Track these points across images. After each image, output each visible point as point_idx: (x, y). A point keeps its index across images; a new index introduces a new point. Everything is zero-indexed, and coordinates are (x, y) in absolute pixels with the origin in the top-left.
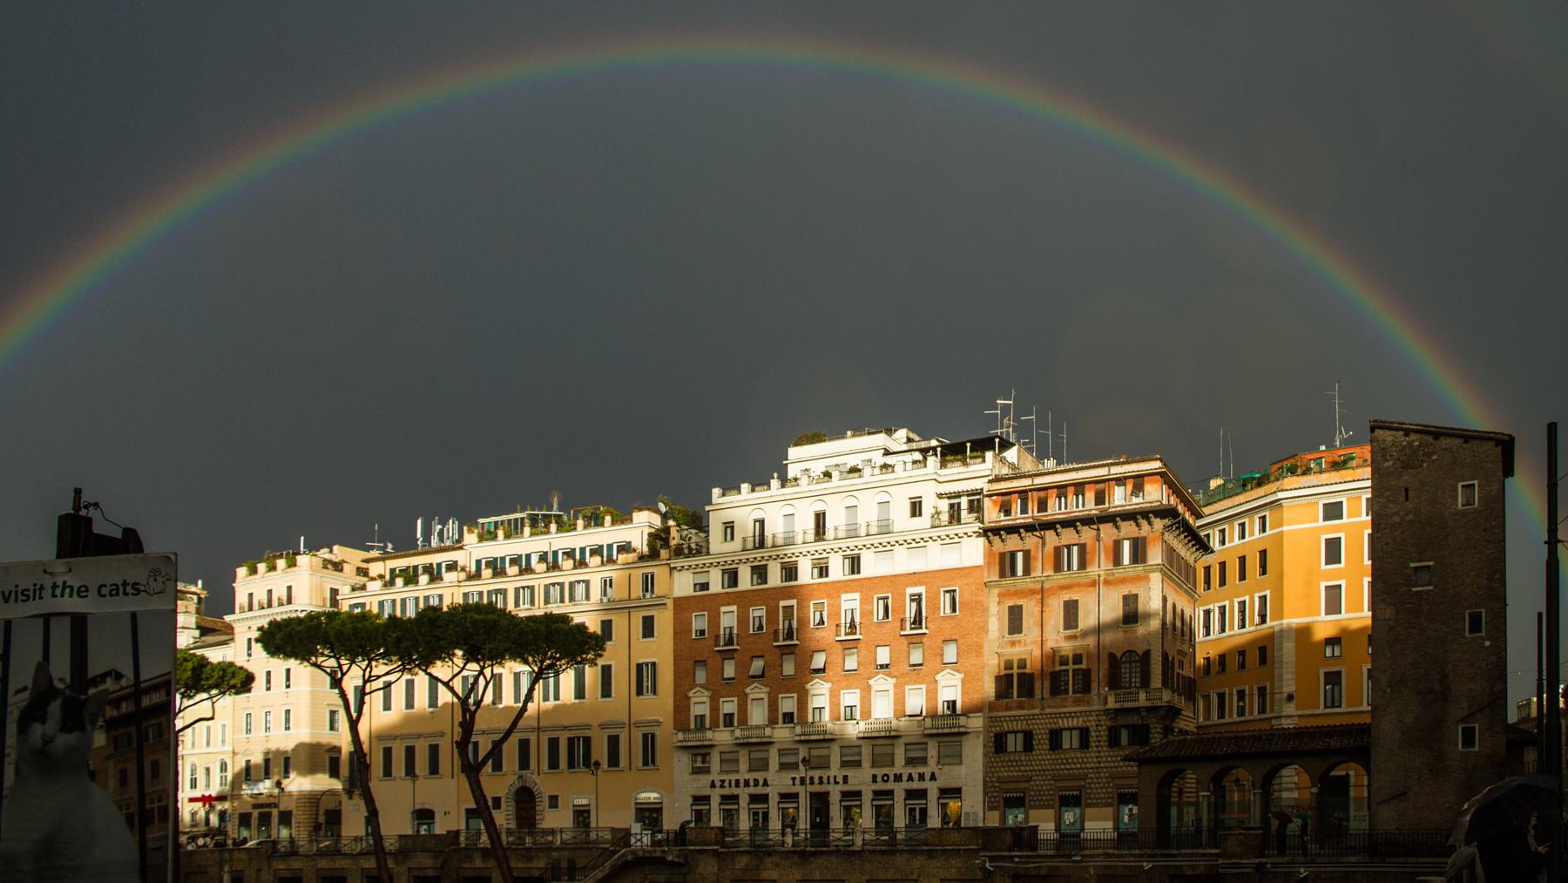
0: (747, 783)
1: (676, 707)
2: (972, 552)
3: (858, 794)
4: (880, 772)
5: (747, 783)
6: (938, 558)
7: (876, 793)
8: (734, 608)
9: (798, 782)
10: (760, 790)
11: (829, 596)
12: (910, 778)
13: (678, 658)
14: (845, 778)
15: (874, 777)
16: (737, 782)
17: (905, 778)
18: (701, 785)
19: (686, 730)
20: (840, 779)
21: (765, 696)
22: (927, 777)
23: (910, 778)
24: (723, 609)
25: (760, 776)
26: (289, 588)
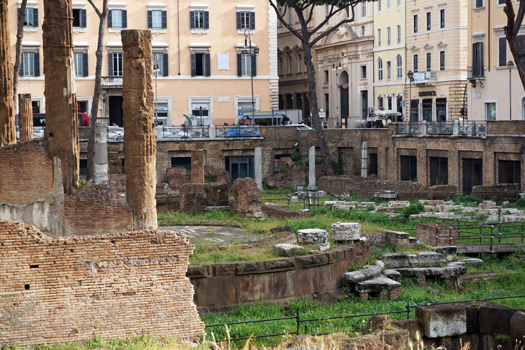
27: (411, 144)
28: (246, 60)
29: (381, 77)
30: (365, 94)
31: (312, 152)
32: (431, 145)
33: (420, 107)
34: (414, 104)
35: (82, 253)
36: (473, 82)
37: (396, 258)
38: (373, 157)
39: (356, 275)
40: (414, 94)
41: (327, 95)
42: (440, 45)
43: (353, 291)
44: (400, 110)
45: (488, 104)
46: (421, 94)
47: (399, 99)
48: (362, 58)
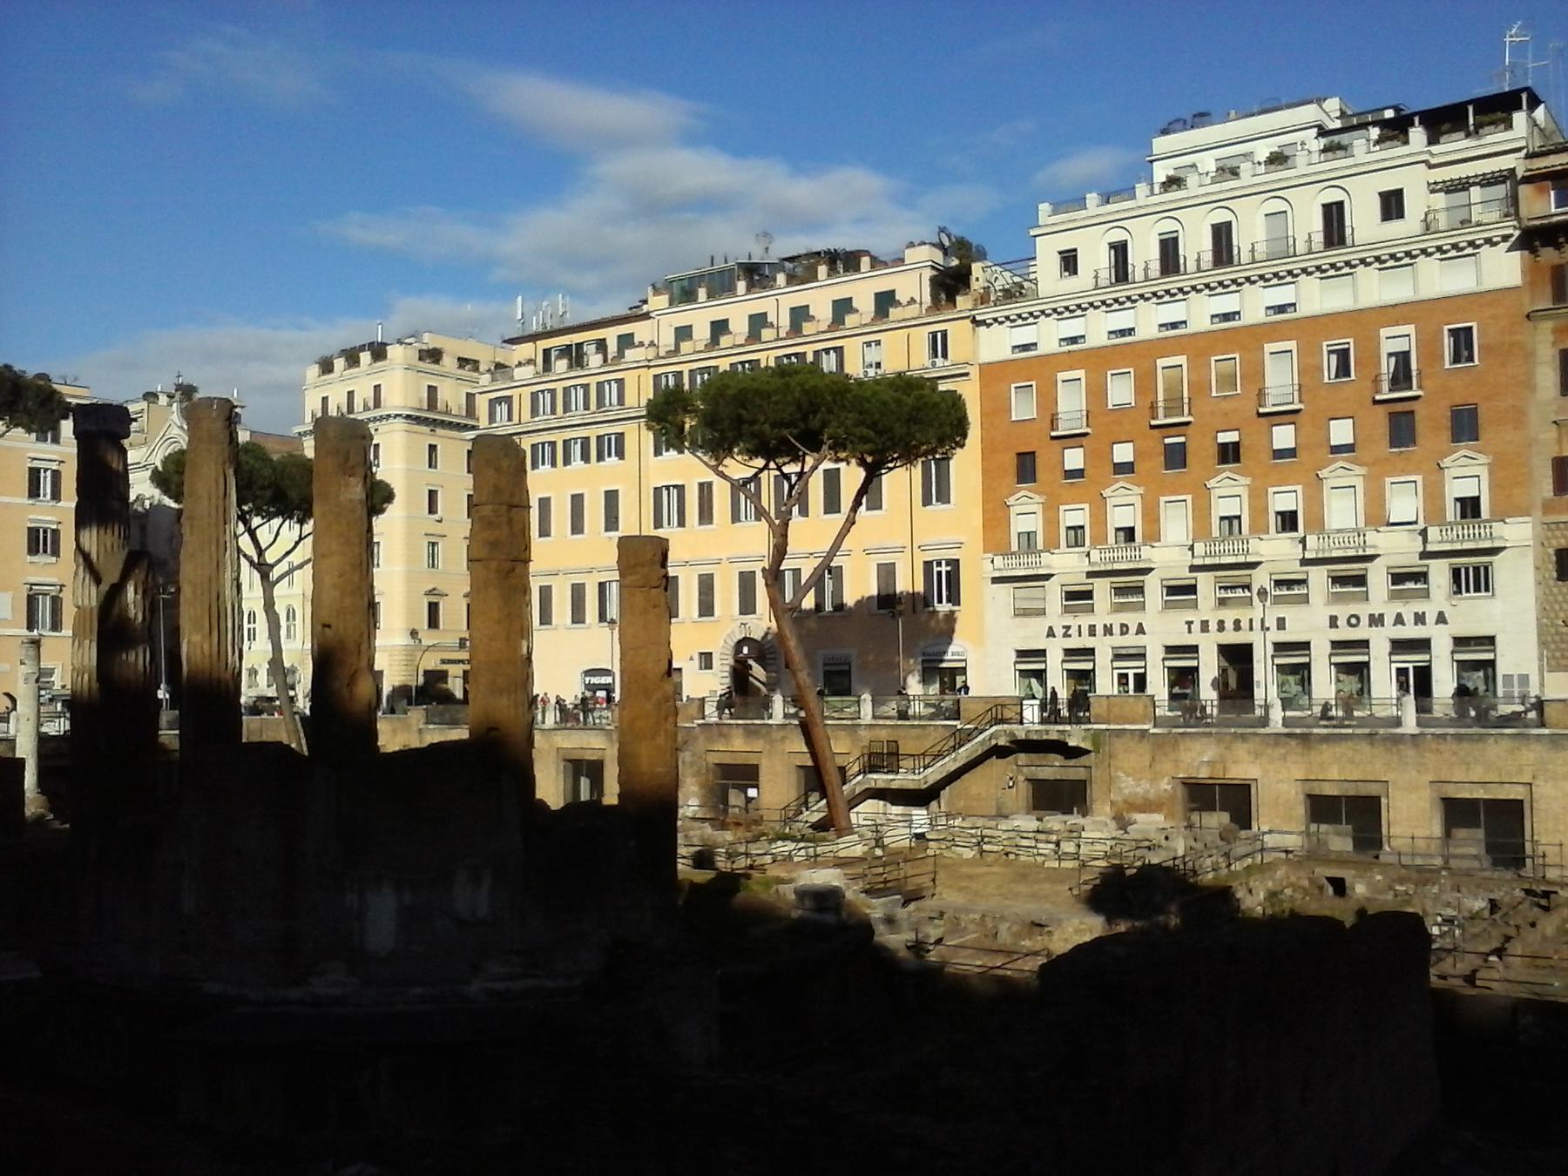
0: (1108, 630)
2: (1504, 268)
3: (1305, 646)
4: (1343, 612)
5: (1108, 630)
6: (1439, 279)
7: (1337, 645)
8: (1080, 374)
9: (1196, 627)
10: (1131, 640)
11: (1242, 348)
12: (1399, 620)
14: (1281, 624)
15: (1333, 622)
16: (1092, 631)
17: (1389, 619)
18: (1031, 634)
19: (1007, 553)
20: (1271, 622)
22: (1431, 618)
23: (1399, 620)
24: (1061, 376)
25: (1132, 619)
26: (377, 388)
28: (45, 607)
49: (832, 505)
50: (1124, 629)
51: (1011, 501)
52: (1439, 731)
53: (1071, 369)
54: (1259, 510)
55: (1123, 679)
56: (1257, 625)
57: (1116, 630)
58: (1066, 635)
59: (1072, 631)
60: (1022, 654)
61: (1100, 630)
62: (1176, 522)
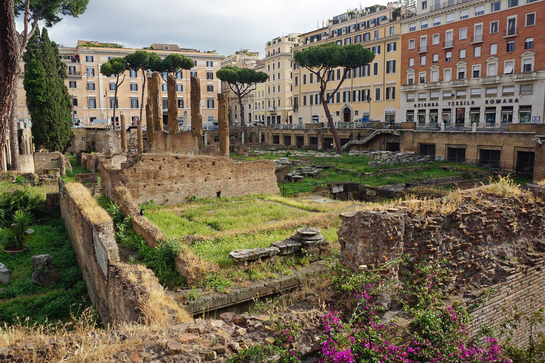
0: (429, 105)
1: (401, 77)
3: (478, 109)
4: (489, 99)
5: (429, 105)
7: (487, 108)
9: (451, 104)
11: (468, 26)
13: (403, 58)
14: (473, 103)
15: (487, 102)
16: (425, 105)
18: (411, 106)
20: (470, 103)
21: (438, 70)
25: (435, 102)
27: (277, 132)
29: (256, 108)
30: (250, 114)
31: (243, 134)
32: (285, 132)
33: (271, 119)
34: (269, 118)
35: (245, 167)
36: (294, 111)
37: (298, 169)
38: (263, 136)
39: (290, 174)
40: (268, 114)
41: (236, 115)
42: (278, 98)
43: (289, 180)
44: (263, 120)
45: (299, 118)
46: (271, 114)
47: (263, 116)
48: (249, 102)
49: (338, 78)
50: (433, 105)
51: (407, 71)
52: (481, 132)
53: (424, 34)
54: (469, 72)
55: (505, 116)
56: (466, 103)
57: (431, 105)
58: (419, 106)
59: (421, 105)
60: (408, 111)
61: (427, 105)
62: (448, 77)
